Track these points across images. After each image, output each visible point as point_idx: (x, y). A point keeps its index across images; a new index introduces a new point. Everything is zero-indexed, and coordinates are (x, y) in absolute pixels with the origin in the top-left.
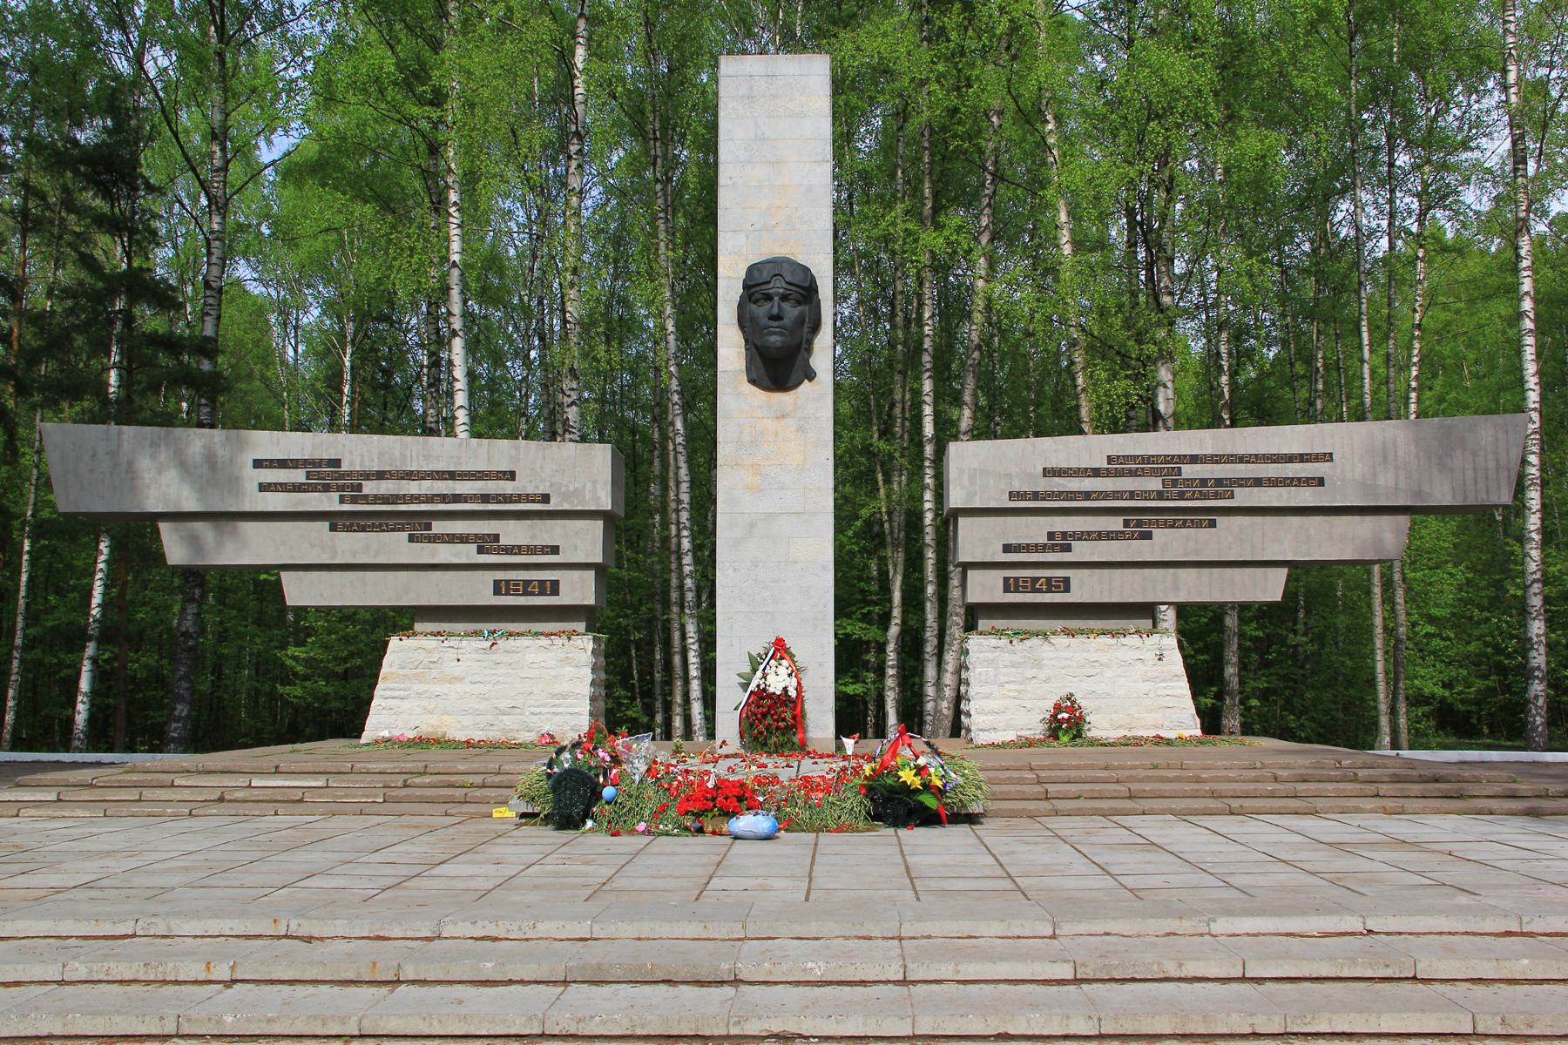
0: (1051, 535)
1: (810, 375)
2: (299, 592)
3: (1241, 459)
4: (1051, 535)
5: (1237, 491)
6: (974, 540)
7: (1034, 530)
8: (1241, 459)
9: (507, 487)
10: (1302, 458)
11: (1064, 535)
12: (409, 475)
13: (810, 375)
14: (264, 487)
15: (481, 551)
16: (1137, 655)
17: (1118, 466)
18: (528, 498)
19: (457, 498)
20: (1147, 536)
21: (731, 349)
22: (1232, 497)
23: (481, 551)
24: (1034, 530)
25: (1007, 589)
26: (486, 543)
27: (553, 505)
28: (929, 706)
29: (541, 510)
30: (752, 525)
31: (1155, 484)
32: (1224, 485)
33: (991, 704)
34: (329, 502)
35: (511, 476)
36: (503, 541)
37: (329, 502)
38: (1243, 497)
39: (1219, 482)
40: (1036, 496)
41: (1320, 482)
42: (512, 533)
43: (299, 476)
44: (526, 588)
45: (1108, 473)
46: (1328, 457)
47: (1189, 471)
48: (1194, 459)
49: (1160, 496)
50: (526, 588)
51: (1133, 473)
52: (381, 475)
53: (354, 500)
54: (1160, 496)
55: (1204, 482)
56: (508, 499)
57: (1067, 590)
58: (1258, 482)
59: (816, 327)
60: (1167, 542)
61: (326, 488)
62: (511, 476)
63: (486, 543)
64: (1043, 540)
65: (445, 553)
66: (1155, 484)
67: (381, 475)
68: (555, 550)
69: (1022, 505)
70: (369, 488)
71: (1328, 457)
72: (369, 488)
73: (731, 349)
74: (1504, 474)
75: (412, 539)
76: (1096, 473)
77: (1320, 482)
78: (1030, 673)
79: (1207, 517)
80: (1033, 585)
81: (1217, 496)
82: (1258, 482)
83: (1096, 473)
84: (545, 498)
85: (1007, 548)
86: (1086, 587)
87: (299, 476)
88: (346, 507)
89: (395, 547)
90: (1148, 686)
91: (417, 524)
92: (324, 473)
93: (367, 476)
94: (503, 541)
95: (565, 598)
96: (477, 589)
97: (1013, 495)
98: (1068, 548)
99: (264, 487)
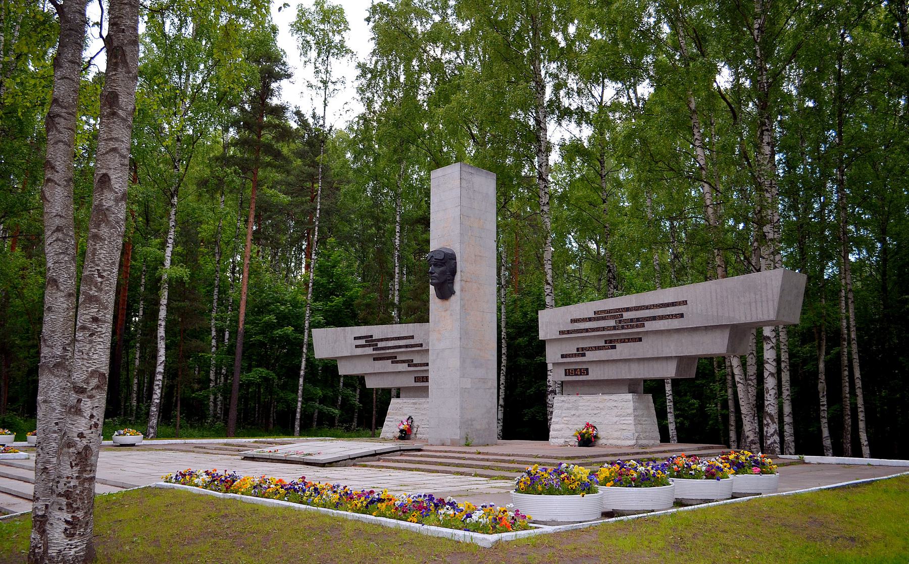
0: (578, 349)
2: (370, 384)
4: (578, 349)
5: (646, 323)
10: (673, 304)
12: (387, 339)
14: (357, 346)
15: (409, 366)
17: (600, 316)
19: (400, 347)
20: (614, 347)
23: (409, 366)
25: (566, 375)
26: (410, 363)
30: (438, 354)
31: (612, 323)
32: (640, 321)
34: (369, 351)
35: (412, 337)
39: (638, 320)
40: (569, 332)
41: (682, 316)
47: (627, 315)
48: (628, 310)
49: (614, 328)
54: (614, 328)
55: (632, 320)
57: (587, 374)
58: (654, 318)
60: (623, 350)
62: (412, 337)
64: (575, 352)
66: (612, 323)
70: (380, 345)
72: (380, 345)
74: (771, 303)
76: (590, 319)
77: (682, 316)
78: (573, 412)
81: (637, 326)
82: (654, 318)
83: (590, 319)
85: (563, 356)
86: (595, 374)
88: (375, 352)
90: (617, 418)
91: (393, 359)
92: (370, 341)
94: (407, 364)
98: (584, 355)
99: (357, 346)
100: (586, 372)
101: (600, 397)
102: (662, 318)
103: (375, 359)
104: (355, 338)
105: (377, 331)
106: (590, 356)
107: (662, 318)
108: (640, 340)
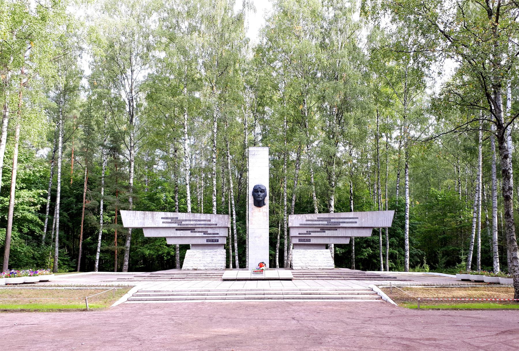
1: (264, 204)
2: (169, 242)
3: (342, 218)
4: (307, 232)
6: (293, 233)
7: (304, 231)
8: (342, 218)
9: (209, 223)
11: (310, 232)
13: (264, 204)
14: (163, 222)
16: (323, 253)
17: (319, 219)
18: (213, 225)
20: (325, 232)
21: (251, 200)
23: (204, 234)
24: (304, 231)
26: (205, 233)
27: (218, 226)
28: (285, 262)
29: (215, 226)
31: (326, 223)
36: (208, 232)
38: (342, 225)
39: (337, 222)
41: (356, 222)
42: (210, 231)
43: (170, 220)
44: (212, 241)
45: (317, 221)
46: (357, 218)
47: (332, 220)
48: (333, 218)
49: (327, 225)
50: (212, 241)
51: (322, 221)
52: (186, 220)
53: (181, 225)
54: (327, 225)
55: (335, 222)
56: (209, 225)
58: (344, 222)
59: (266, 196)
60: (328, 233)
61: (176, 223)
62: (210, 221)
63: (205, 233)
64: (306, 232)
65: (198, 235)
66: (326, 223)
67: (186, 220)
68: (218, 234)
69: (301, 227)
70: (183, 223)
71: (357, 218)
72: (183, 223)
73: (251, 200)
74: (390, 221)
75: (191, 232)
76: (315, 221)
77: (356, 222)
78: (303, 256)
79: (335, 229)
80: (304, 241)
82: (344, 222)
83: (315, 221)
84: (216, 225)
85: (299, 234)
86: (313, 241)
87: (170, 220)
88: (179, 226)
89: (188, 233)
91: (192, 230)
92: (175, 220)
93: (183, 220)
94: (208, 232)
95: (219, 243)
96: (204, 241)
97: (300, 224)
98: (310, 234)
99: (163, 222)
100: (310, 241)
101: (316, 251)
102: (348, 223)
103: (176, 230)
104: (162, 218)
105: (181, 216)
106: (313, 234)
107: (348, 223)
108: (336, 230)
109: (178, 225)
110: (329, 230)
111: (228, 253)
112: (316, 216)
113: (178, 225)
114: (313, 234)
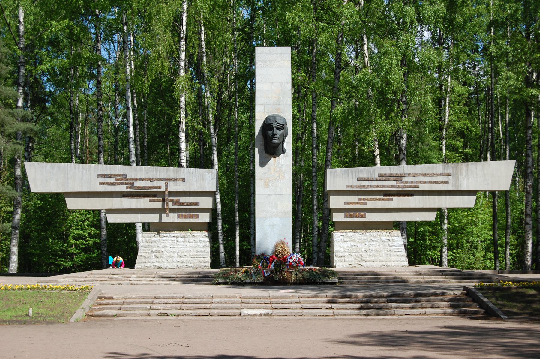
5: (420, 185)
6: (335, 202)
7: (355, 199)
14: (101, 184)
17: (382, 177)
20: (392, 200)
22: (365, 217)
31: (393, 183)
33: (340, 254)
37: (123, 188)
38: (422, 187)
41: (447, 182)
43: (112, 180)
46: (449, 175)
47: (405, 179)
60: (397, 202)
61: (122, 184)
66: (393, 183)
70: (137, 184)
71: (449, 175)
72: (137, 184)
75: (150, 201)
85: (346, 203)
86: (371, 217)
87: (112, 180)
88: (129, 190)
92: (122, 179)
93: (137, 180)
97: (348, 187)
99: (101, 184)
109: (127, 188)
110: (380, 200)
111: (214, 240)
112: (379, 169)
113: (127, 188)
114: (370, 205)
